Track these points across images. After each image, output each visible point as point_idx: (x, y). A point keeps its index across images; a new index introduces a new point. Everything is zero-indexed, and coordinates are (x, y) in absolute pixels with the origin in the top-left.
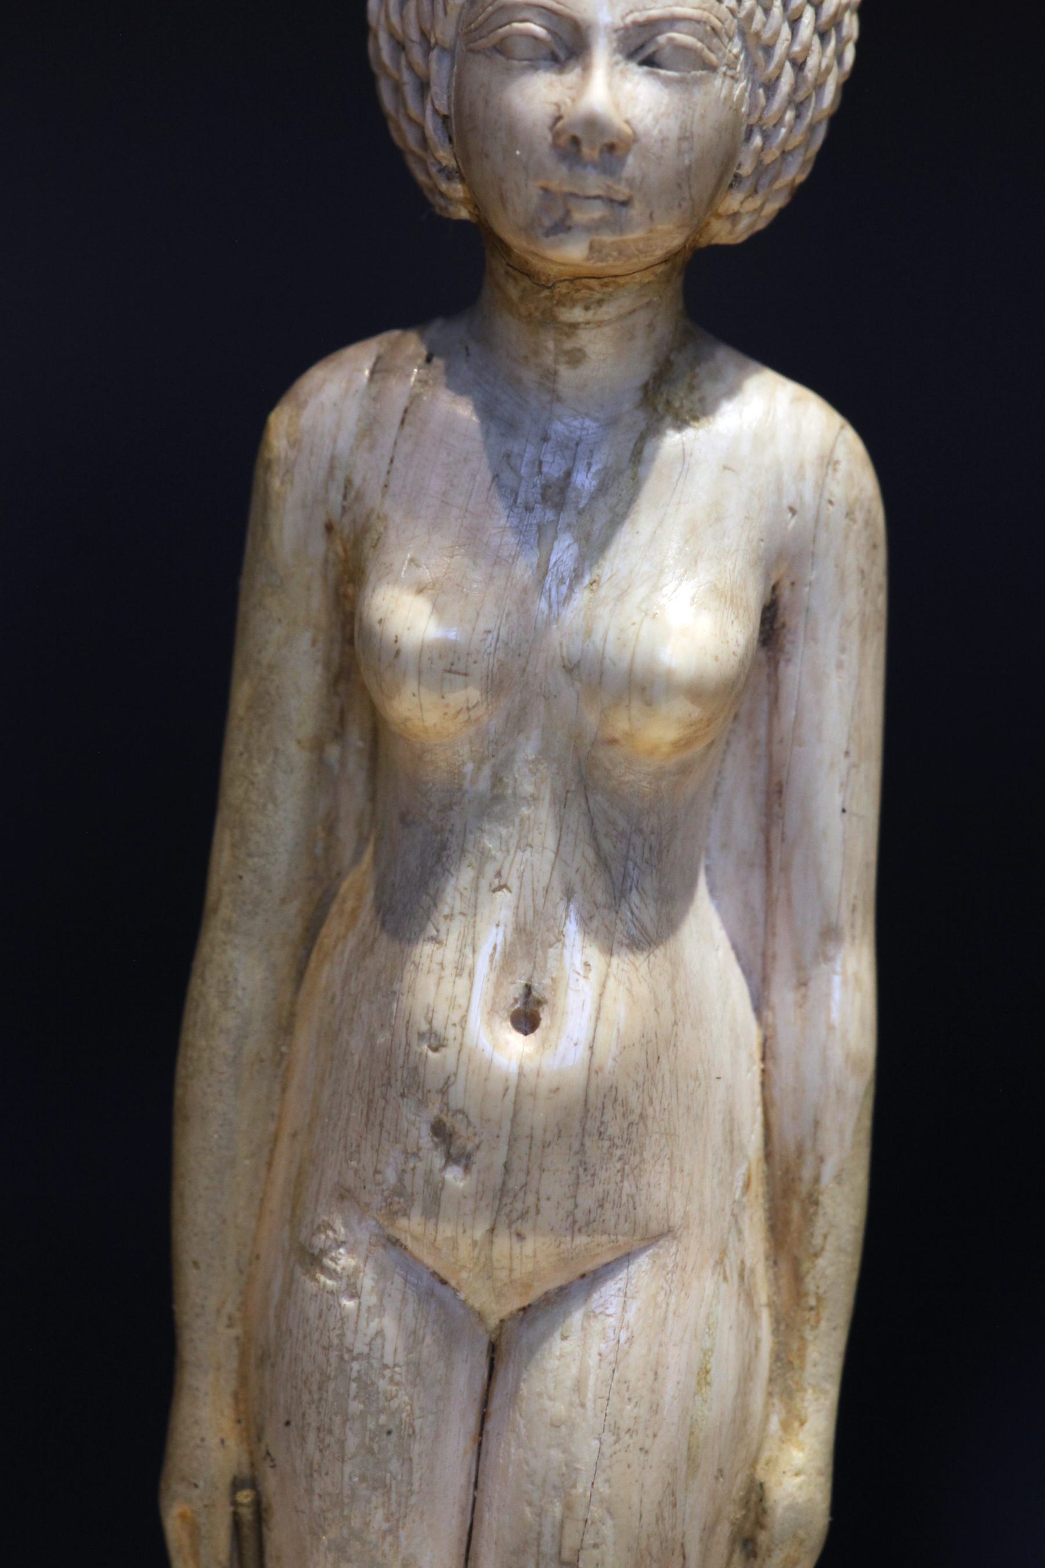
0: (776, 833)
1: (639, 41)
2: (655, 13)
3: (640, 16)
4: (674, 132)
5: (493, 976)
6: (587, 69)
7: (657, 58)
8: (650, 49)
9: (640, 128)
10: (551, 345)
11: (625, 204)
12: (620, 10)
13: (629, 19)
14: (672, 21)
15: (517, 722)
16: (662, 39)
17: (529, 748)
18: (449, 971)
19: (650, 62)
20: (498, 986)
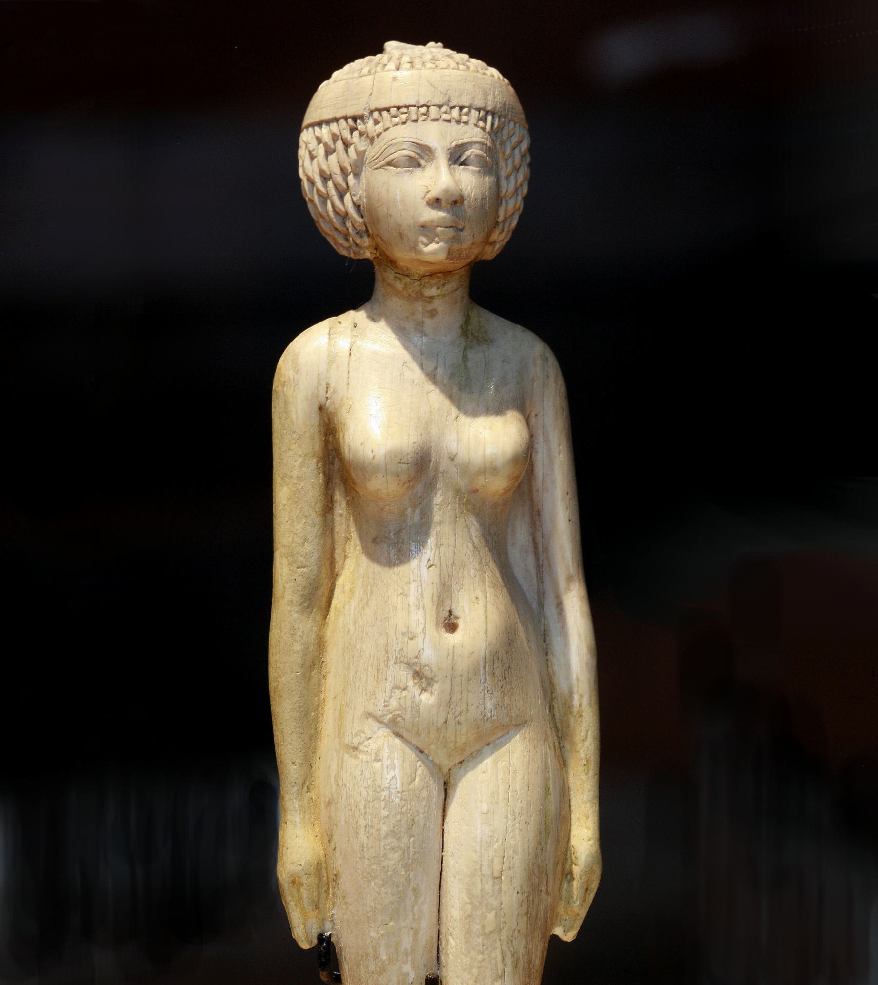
0: (539, 535)
1: (458, 155)
2: (465, 141)
3: (460, 142)
4: (480, 196)
5: (435, 608)
6: (437, 168)
7: (467, 162)
8: (463, 159)
9: (466, 193)
10: (420, 309)
11: (462, 230)
12: (448, 140)
13: (453, 144)
14: (470, 144)
15: (431, 487)
16: (468, 153)
17: (438, 499)
18: (413, 608)
19: (463, 164)
20: (437, 612)
